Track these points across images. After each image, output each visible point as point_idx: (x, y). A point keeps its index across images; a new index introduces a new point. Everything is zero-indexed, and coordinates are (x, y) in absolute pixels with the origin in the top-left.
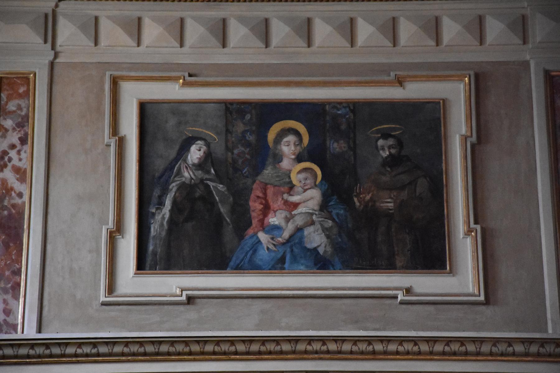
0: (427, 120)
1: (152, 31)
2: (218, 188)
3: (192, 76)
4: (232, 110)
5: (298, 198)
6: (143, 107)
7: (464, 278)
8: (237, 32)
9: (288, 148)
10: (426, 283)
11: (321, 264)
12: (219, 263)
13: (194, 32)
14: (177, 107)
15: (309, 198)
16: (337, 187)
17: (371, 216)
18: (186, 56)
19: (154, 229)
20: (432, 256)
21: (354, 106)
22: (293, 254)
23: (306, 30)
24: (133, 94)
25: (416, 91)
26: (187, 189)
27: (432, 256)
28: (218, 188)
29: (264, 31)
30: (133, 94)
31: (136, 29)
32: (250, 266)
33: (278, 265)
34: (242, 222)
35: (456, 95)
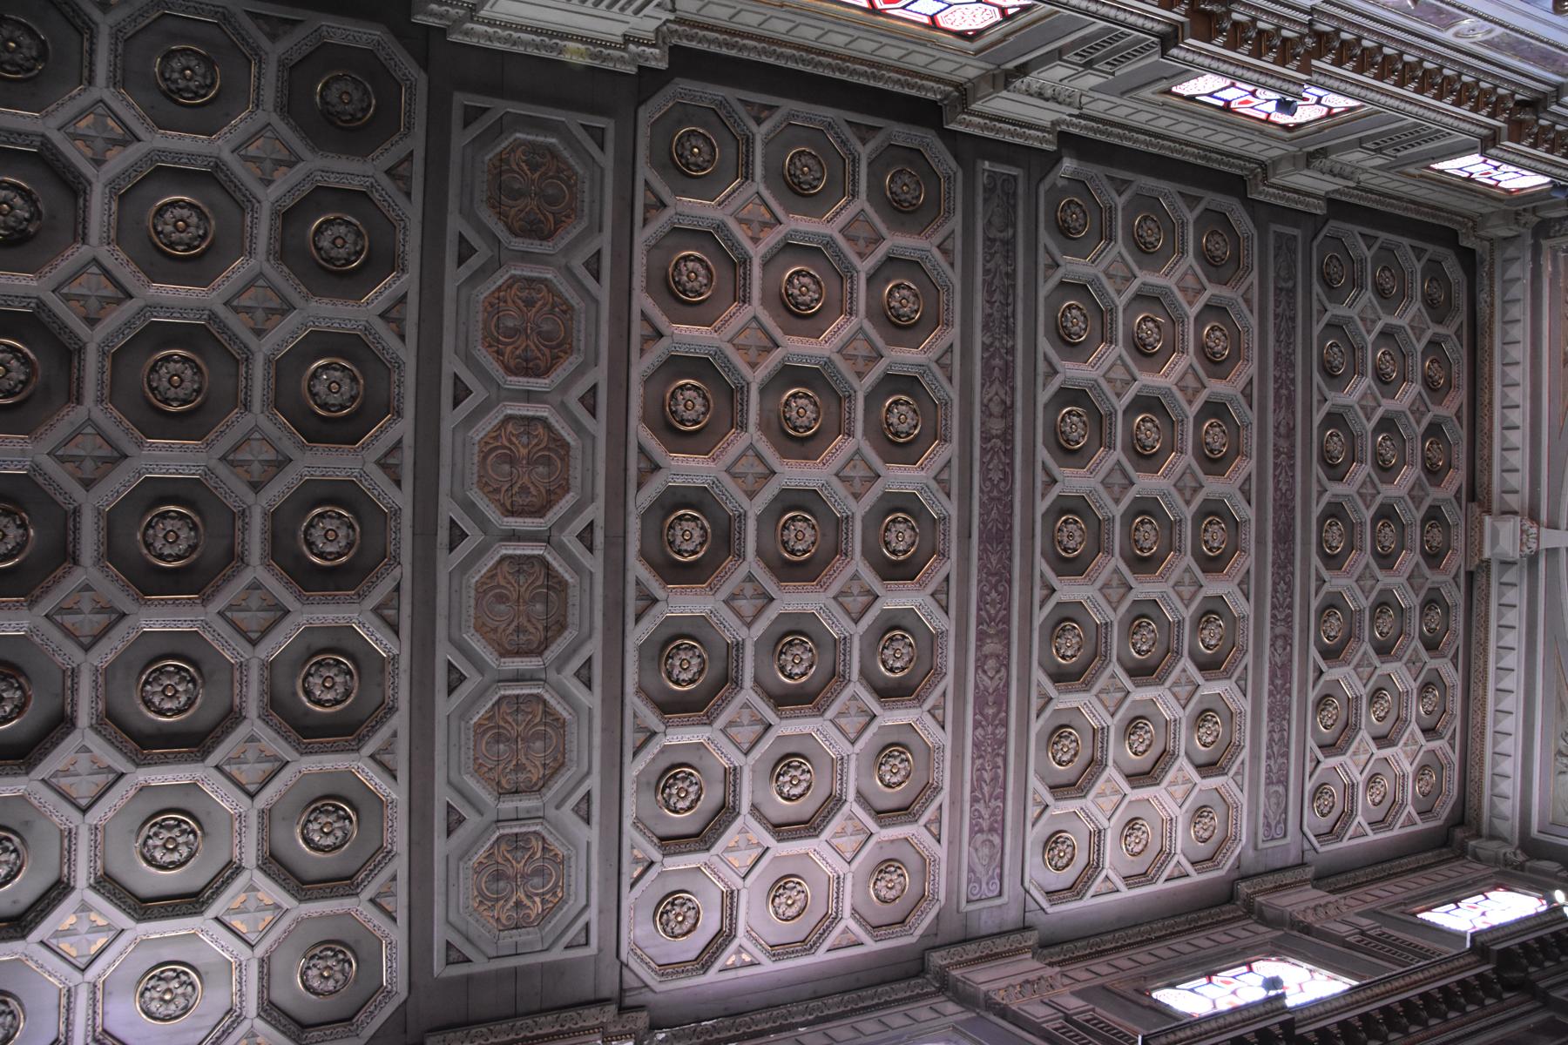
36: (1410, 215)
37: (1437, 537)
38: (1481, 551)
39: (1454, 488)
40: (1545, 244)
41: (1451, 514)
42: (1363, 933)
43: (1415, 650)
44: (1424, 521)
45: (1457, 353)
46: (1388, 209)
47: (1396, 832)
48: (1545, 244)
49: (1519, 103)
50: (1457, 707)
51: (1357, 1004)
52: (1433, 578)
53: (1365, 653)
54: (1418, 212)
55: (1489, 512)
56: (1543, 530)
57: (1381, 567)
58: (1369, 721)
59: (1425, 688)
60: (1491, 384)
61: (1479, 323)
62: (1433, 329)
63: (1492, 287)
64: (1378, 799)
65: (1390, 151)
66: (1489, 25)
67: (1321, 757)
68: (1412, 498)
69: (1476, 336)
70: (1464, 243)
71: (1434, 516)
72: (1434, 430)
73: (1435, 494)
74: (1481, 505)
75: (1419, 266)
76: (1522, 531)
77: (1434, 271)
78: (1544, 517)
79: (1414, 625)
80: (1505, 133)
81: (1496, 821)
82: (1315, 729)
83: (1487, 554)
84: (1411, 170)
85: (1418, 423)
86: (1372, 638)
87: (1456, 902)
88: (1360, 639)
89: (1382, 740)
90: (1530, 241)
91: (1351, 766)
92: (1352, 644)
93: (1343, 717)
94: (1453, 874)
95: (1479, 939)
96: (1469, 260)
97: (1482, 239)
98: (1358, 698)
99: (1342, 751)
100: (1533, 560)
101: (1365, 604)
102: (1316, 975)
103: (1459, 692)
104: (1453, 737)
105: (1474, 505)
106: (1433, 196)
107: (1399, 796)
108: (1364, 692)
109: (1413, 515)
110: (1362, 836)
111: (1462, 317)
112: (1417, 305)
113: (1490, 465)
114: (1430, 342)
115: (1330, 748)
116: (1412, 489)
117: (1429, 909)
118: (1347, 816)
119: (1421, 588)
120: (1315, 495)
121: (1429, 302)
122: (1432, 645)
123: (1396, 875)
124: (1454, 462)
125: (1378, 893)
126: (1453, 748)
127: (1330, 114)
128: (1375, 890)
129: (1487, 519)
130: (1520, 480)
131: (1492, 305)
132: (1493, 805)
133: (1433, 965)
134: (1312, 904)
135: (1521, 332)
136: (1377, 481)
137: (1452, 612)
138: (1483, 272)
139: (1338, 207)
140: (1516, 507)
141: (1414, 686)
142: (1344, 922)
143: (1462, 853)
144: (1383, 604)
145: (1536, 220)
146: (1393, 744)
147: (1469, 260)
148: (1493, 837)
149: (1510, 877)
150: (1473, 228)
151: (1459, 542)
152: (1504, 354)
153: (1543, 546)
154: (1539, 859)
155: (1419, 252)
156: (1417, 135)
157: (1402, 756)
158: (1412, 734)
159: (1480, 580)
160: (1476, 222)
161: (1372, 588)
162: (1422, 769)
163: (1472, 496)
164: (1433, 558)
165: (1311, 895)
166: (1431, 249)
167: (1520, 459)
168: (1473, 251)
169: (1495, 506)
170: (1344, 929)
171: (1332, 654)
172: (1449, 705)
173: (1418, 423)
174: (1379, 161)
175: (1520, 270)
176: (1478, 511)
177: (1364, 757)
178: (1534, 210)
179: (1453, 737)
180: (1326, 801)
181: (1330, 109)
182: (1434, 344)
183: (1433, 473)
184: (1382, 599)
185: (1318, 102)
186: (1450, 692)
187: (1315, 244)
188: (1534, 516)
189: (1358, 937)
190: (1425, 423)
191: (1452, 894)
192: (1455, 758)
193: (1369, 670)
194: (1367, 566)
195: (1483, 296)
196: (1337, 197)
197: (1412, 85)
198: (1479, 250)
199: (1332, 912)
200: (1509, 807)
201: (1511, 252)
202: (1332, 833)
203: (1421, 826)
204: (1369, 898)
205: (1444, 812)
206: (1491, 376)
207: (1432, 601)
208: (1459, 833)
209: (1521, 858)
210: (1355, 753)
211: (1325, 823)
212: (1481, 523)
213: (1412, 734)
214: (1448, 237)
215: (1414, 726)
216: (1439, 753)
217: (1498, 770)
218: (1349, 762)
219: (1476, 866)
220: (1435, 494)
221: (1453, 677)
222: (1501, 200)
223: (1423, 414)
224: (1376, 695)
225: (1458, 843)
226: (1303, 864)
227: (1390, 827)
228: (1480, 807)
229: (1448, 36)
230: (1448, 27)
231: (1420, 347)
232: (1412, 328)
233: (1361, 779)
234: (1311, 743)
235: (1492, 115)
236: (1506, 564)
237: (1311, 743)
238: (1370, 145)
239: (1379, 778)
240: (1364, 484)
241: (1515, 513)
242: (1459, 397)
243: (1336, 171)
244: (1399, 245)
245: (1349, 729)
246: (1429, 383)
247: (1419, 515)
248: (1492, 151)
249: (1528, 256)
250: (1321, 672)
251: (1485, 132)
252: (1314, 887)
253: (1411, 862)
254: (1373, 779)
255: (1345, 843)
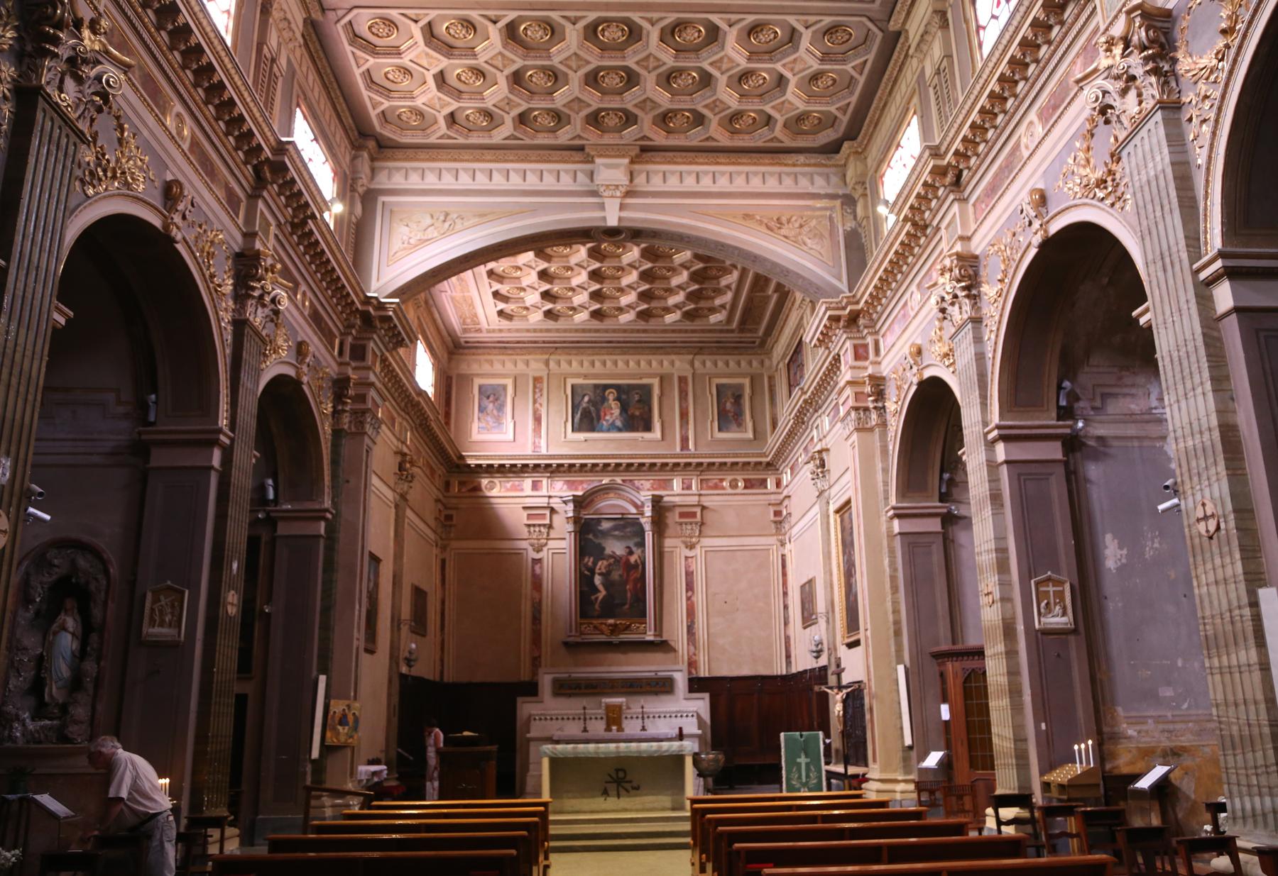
0: (647, 389)
1: (574, 364)
2: (592, 409)
3: (586, 376)
4: (596, 386)
5: (613, 412)
6: (573, 386)
7: (656, 434)
8: (597, 364)
9: (611, 397)
10: (647, 435)
11: (620, 430)
12: (592, 429)
13: (586, 364)
14: (581, 386)
15: (616, 412)
16: (624, 409)
17: (633, 417)
18: (583, 371)
19: (576, 420)
20: (648, 427)
21: (629, 385)
22: (613, 428)
23: (615, 363)
24: (570, 382)
25: (645, 381)
26: (584, 409)
27: (648, 427)
28: (592, 409)
29: (604, 364)
30: (570, 382)
31: (570, 363)
32: (601, 431)
33: (608, 431)
34: (599, 419)
35: (655, 382)
36: (875, 102)
37: (612, 121)
38: (601, 156)
39: (651, 135)
40: (838, 203)
41: (631, 132)
42: (273, 60)
43: (519, 105)
44: (624, 111)
45: (759, 139)
46: (883, 85)
47: (365, 94)
48: (838, 203)
49: (961, 171)
50: (475, 139)
51: (210, 43)
52: (578, 119)
53: (514, 62)
54: (876, 108)
55: (632, 162)
56: (619, 201)
57: (587, 75)
58: (456, 67)
59: (488, 114)
60: (734, 164)
61: (781, 156)
62: (780, 119)
63: (809, 165)
64: (390, 76)
65: (936, 80)
66: (1032, 147)
67: (421, 23)
68: (644, 101)
69: (774, 152)
70: (846, 144)
71: (629, 119)
72: (699, 119)
73: (646, 119)
74: (637, 156)
75: (833, 109)
76: (617, 186)
77: (829, 121)
78: (629, 201)
79: (540, 104)
80: (939, 162)
81: (386, 172)
82: (445, 18)
83: (598, 161)
84: (915, 100)
85: (706, 106)
86: (526, 68)
87: (316, 139)
88: (525, 57)
89: (441, 79)
90: (840, 192)
91: (416, 51)
92: (521, 51)
93: (458, 43)
94: (338, 139)
95: (290, 148)
96: (833, 148)
97: (847, 159)
98: (475, 56)
99: (428, 44)
100: (595, 193)
101: (556, 61)
102: (226, 15)
103: (487, 141)
104: (450, 137)
105: (637, 150)
106: (893, 109)
107: (393, 94)
108: (480, 61)
109: (630, 100)
110: (358, 65)
111: (788, 143)
112: (802, 106)
113: (669, 163)
114: (770, 117)
115: (430, 32)
116: (652, 101)
117: (305, 117)
118: (372, 49)
119: (571, 109)
120: (649, 15)
121: (801, 118)
122: (522, 119)
123: (328, 93)
124: (671, 136)
125: (311, 78)
126: (441, 138)
127: (979, 28)
128: (312, 76)
129: (626, 161)
130: (657, 184)
131: (794, 165)
132: (398, 169)
133: (260, 111)
134: (289, 16)
135: (772, 185)
136: (661, 70)
137: (551, 135)
138: (821, 159)
139: (893, 40)
140: (636, 181)
141: (489, 104)
142: (279, 44)
143: (356, 147)
144: (555, 77)
145: (856, 196)
146: (439, 88)
147: (833, 148)
148: (373, 170)
149: (347, 184)
150: (857, 152)
151: (608, 139)
152: (756, 174)
153: (606, 200)
154: (362, 203)
155: (843, 110)
156: (945, 98)
157: (430, 96)
158: (449, 104)
159: (578, 156)
160: (861, 154)
161: (570, 68)
162: (420, 114)
163: (644, 150)
164: (595, 119)
165: (298, 17)
166: (845, 119)
167: (673, 184)
168: (837, 151)
169: (637, 167)
170: (273, 40)
171: (511, 32)
172: (475, 134)
173: (706, 106)
174: (929, 72)
175: (820, 185)
176: (633, 154)
177: (425, 64)
178: (865, 195)
179: (450, 137)
180: (383, 30)
181: (984, 28)
182: (769, 120)
183: (664, 119)
184: (560, 77)
185: (994, 17)
186: (486, 134)
187: (864, 19)
188: (629, 194)
189: (268, 56)
190: (706, 112)
191: (322, 135)
192: (433, 140)
193: (500, 66)
194: (588, 62)
195: (801, 158)
196: (901, 40)
197: (997, 89)
198: (838, 156)
199: (286, 35)
200: (398, 181)
201: (834, 179)
202: (355, 38)
203: (373, 114)
204: (304, 69)
205: (387, 132)
206: (739, 164)
207: (559, 118)
208: (371, 144)
209: (361, 190)
210: (427, 54)
211: (363, 29)
212: (623, 156)
213: (449, 104)
214: (852, 133)
215: (454, 105)
216: (435, 127)
217: (427, 172)
218: (419, 50)
219: (348, 158)
220: (646, 119)
221: (498, 136)
222: (876, 171)
223: (712, 110)
224: (479, 73)
225: (366, 142)
226: (323, 10)
227: (368, 88)
228: (395, 160)
229: (1032, 116)
230: (1040, 116)
231: (768, 109)
232: (783, 103)
233: (405, 61)
234: (433, 14)
235: (957, 153)
236: (591, 175)
237: (433, 14)
238: (945, 63)
239: (408, 76)
240: (657, 59)
241: (631, 181)
242: (724, 140)
243: (926, 37)
244: (852, 93)
245: (448, 49)
246: (736, 116)
247: (629, 107)
248: (927, 153)
249: (830, 191)
250: (495, 22)
251: (943, 149)
252: (305, 21)
253: (342, 106)
254: (407, 71)
255: (348, 48)
